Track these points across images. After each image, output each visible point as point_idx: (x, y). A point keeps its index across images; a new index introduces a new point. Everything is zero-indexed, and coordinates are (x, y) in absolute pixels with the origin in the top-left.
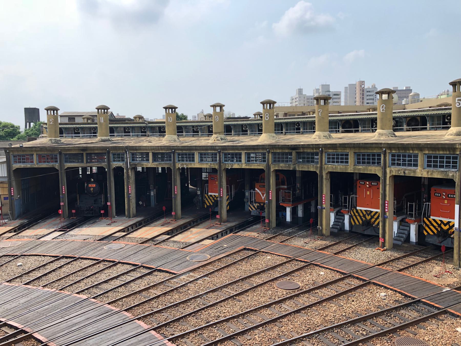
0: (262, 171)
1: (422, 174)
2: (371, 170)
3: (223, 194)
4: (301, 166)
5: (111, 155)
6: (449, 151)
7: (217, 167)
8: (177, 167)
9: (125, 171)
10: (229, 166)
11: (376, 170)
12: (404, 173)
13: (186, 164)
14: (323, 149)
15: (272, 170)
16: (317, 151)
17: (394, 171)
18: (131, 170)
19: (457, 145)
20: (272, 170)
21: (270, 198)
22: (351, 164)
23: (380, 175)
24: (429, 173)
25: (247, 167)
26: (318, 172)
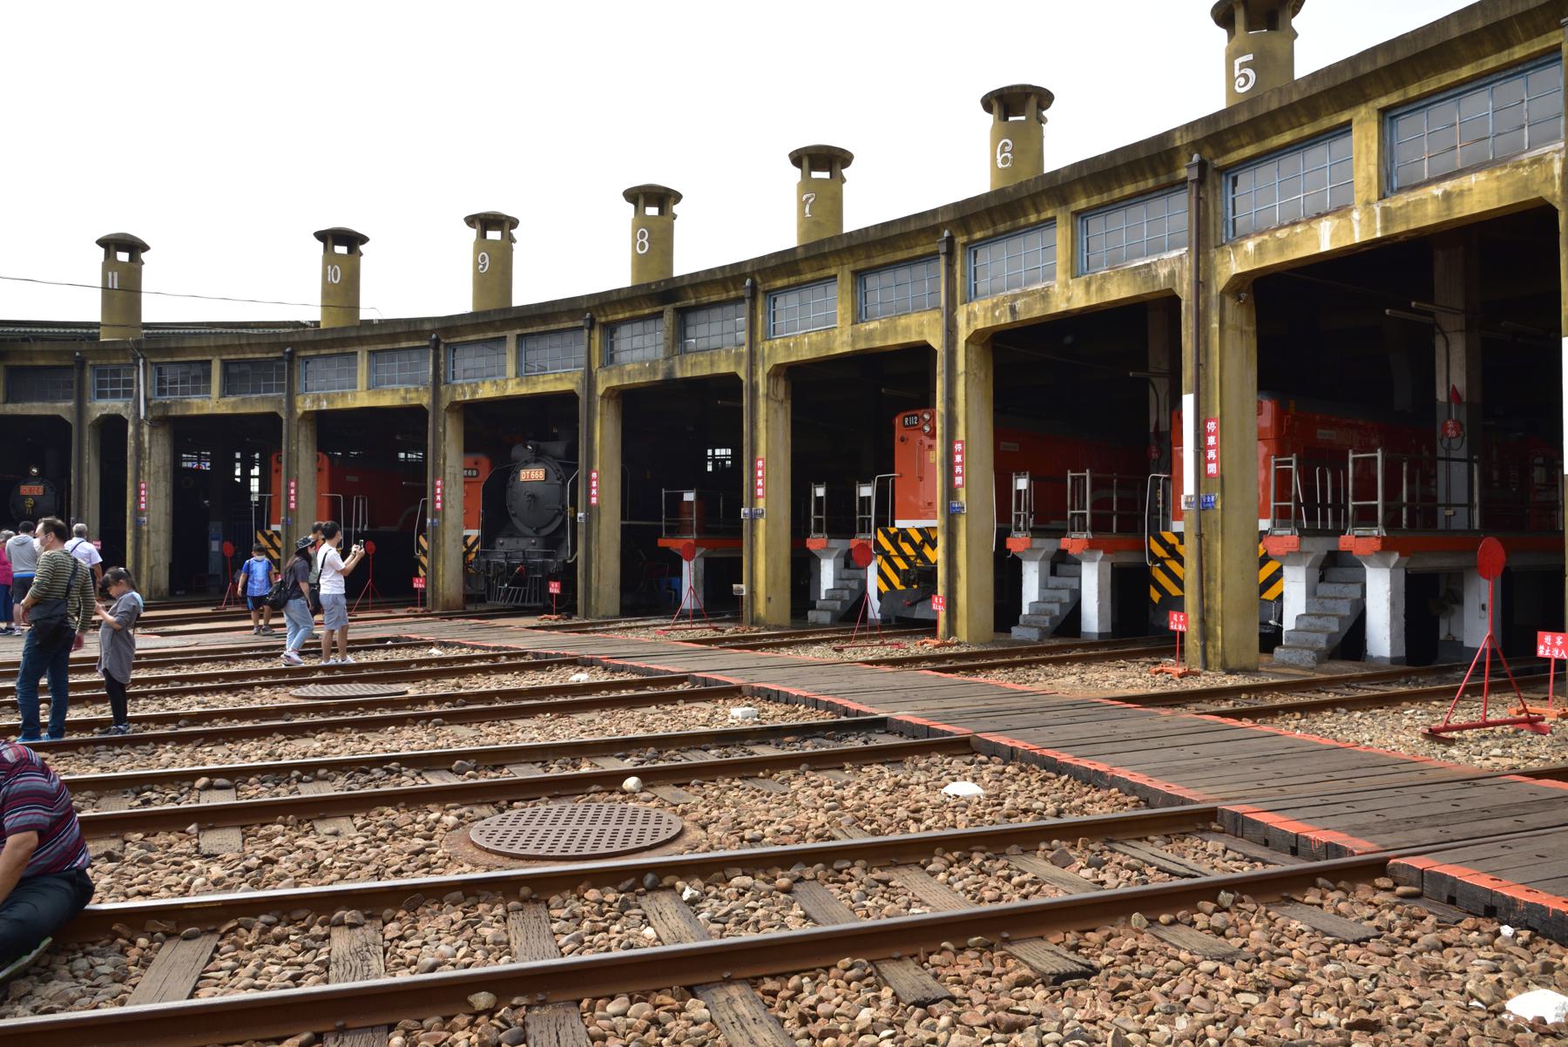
0: (568, 398)
1: (1069, 300)
2: (907, 329)
3: (443, 501)
4: (690, 359)
5: (89, 374)
6: (1156, 175)
7: (425, 400)
8: (300, 411)
9: (131, 429)
10: (464, 394)
11: (921, 324)
12: (1013, 310)
13: (327, 397)
14: (758, 280)
15: (600, 390)
16: (741, 293)
17: (980, 314)
18: (153, 427)
19: (1178, 134)
20: (600, 390)
21: (594, 500)
22: (843, 320)
23: (937, 342)
24: (1093, 288)
25: (523, 390)
26: (742, 375)
